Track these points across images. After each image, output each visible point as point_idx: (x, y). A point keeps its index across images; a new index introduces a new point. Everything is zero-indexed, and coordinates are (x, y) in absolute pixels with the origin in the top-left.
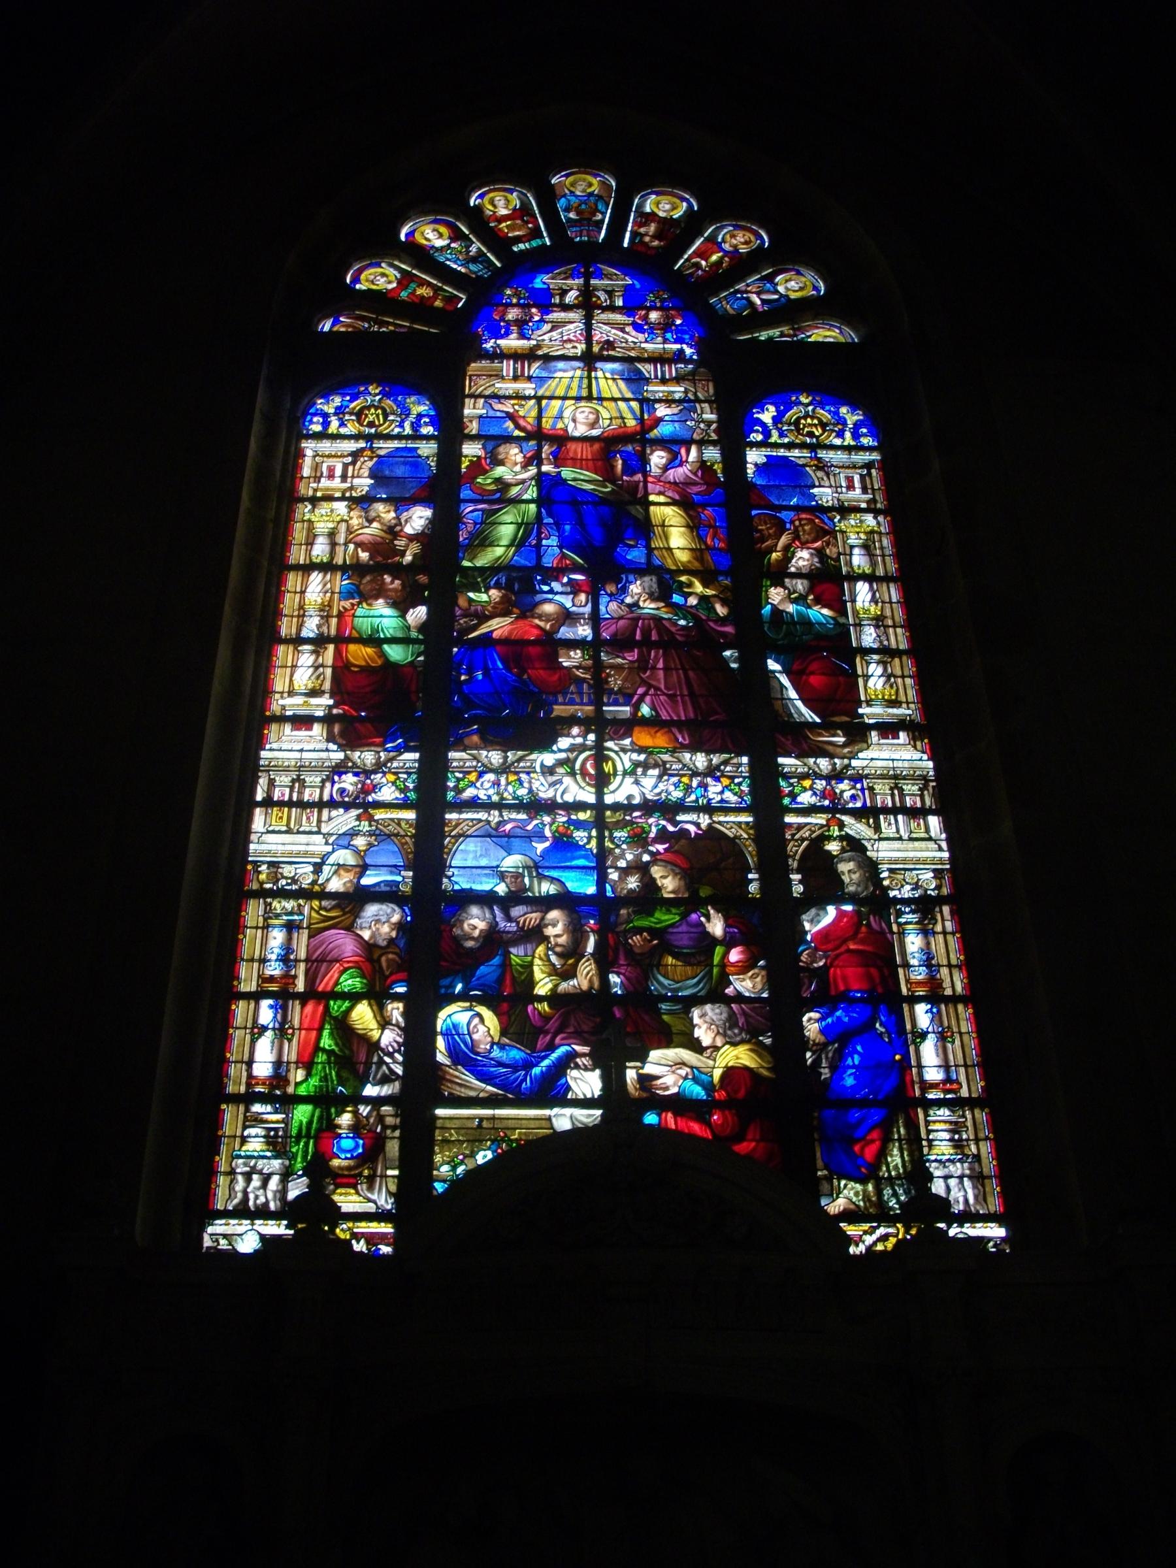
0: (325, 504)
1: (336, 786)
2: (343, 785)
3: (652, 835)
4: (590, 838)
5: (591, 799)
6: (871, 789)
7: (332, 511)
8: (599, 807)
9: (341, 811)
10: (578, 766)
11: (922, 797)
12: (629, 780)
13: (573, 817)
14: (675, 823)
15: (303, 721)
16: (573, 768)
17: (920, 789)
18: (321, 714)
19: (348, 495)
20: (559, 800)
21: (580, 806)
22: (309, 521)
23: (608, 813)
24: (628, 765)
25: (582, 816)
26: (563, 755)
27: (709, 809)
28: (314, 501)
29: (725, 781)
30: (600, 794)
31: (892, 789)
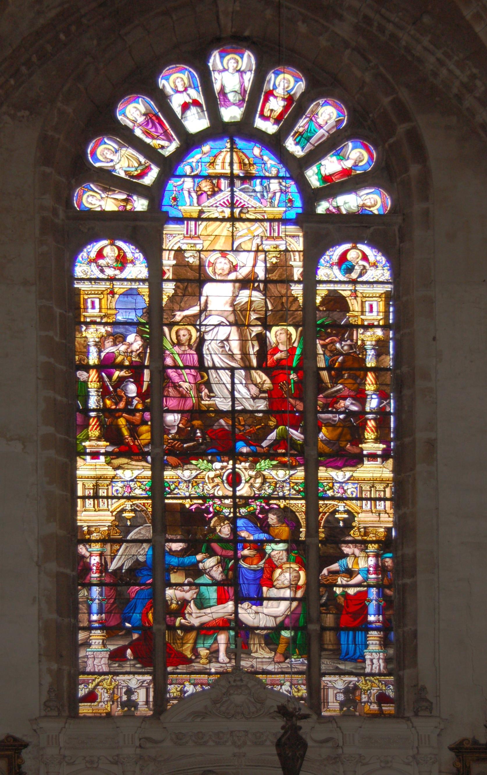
0: (92, 326)
1: (114, 489)
2: (117, 488)
3: (258, 511)
4: (230, 513)
5: (230, 494)
7: (97, 330)
8: (234, 497)
9: (116, 500)
10: (224, 478)
12: (247, 485)
14: (268, 504)
15: (95, 455)
16: (222, 479)
18: (103, 451)
19: (104, 320)
20: (216, 495)
21: (227, 497)
22: (86, 337)
23: (237, 500)
24: (247, 477)
25: (228, 501)
27: (284, 498)
28: (87, 324)
29: (292, 485)
30: (234, 491)
31: (371, 487)
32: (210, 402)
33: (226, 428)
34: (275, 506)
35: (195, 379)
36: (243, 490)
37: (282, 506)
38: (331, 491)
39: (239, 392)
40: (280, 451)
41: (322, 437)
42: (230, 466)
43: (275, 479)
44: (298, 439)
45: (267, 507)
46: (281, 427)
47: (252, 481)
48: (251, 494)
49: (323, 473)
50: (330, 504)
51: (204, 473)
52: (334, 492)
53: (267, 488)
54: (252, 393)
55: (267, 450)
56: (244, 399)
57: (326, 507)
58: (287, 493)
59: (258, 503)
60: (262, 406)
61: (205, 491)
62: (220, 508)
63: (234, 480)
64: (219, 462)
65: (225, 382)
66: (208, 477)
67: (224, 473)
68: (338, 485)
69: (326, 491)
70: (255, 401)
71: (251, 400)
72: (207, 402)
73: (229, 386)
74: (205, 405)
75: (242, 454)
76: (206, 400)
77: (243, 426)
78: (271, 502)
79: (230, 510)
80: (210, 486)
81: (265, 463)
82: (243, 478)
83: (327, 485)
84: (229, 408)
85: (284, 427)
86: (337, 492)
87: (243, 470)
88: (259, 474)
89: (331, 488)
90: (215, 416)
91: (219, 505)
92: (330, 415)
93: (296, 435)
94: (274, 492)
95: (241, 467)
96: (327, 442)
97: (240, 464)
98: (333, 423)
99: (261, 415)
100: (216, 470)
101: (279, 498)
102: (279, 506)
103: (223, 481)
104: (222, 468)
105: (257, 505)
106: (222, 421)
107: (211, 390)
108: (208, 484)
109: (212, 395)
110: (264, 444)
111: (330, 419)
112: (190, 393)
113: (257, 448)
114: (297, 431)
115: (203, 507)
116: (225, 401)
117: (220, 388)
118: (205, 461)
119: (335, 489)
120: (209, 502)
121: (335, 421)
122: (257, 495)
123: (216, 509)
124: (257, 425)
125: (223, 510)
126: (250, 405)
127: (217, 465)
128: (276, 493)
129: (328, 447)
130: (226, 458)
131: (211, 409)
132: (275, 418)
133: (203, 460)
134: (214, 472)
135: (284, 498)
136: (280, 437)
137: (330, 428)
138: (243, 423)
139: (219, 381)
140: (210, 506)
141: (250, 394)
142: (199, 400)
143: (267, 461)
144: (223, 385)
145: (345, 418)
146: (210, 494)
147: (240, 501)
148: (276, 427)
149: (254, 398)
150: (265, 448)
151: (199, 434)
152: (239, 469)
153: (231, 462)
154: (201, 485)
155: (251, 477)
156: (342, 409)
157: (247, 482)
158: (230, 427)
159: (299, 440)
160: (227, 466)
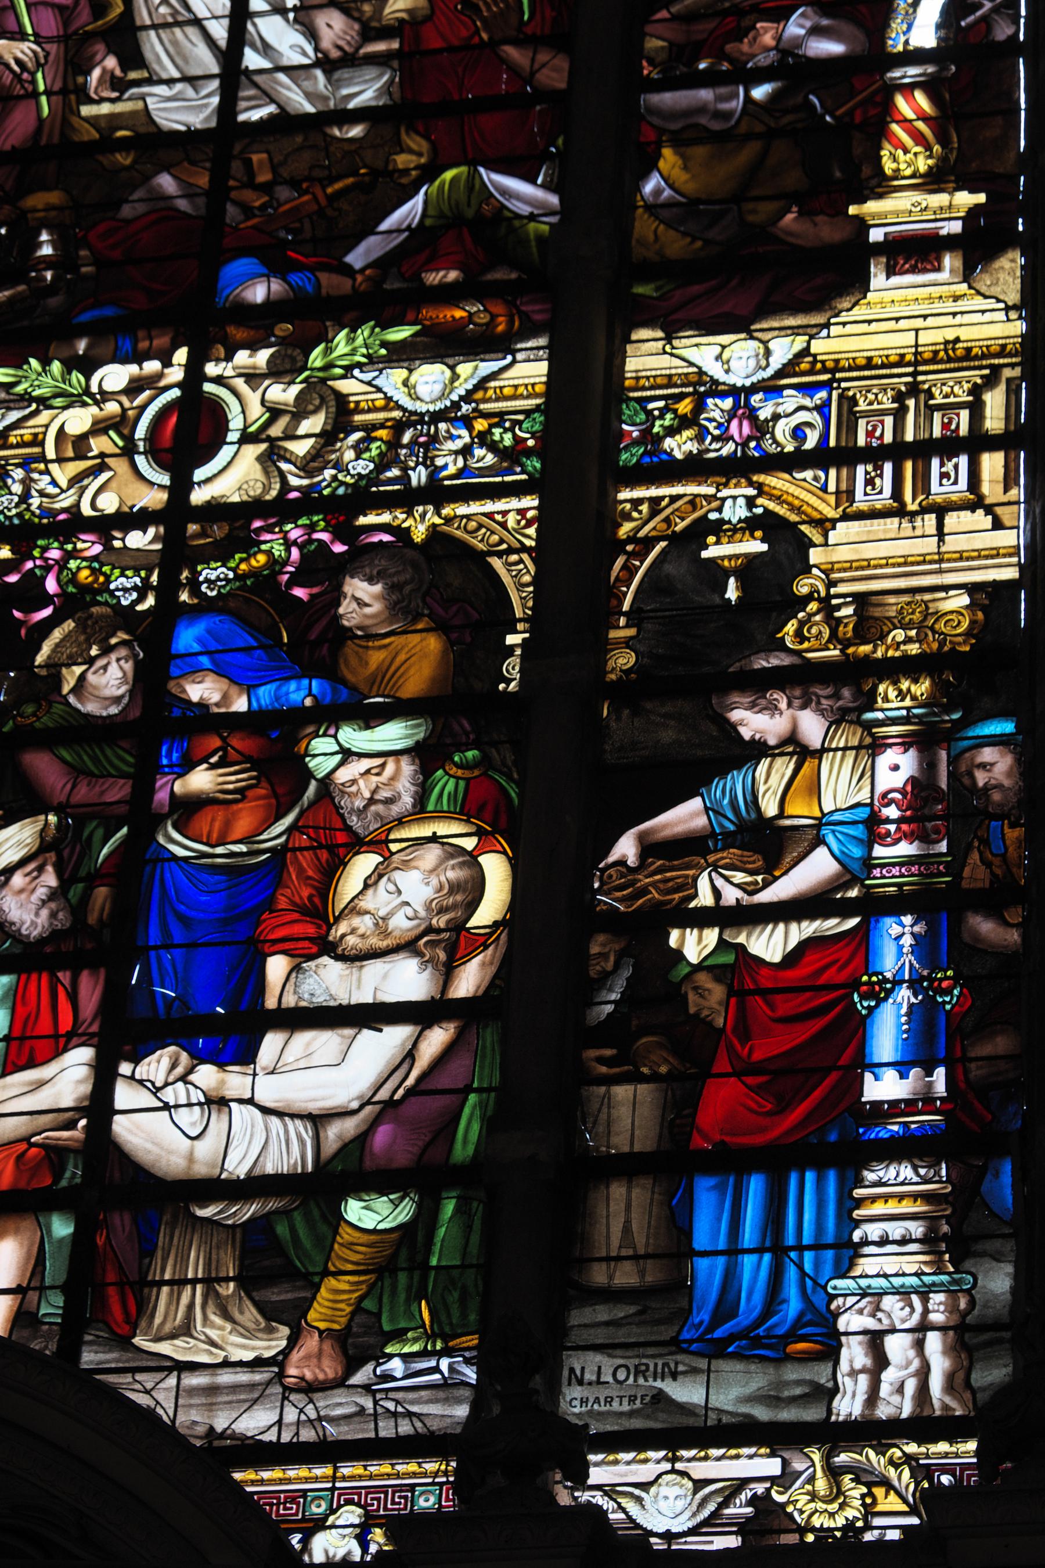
6: (848, 402)
11: (976, 408)
13: (117, 544)
17: (976, 391)
20: (86, 511)
24: (256, 411)
25: (136, 540)
26: (112, 407)
27: (437, 493)
30: (181, 486)
31: (899, 398)
32: (120, 107)
33: (182, 204)
34: (386, 538)
35: (66, 24)
36: (231, 476)
37: (419, 533)
38: (687, 433)
39: (266, 49)
40: (433, 278)
41: (657, 192)
42: (175, 374)
43: (399, 407)
44: (525, 210)
45: (339, 548)
46: (449, 175)
47: (276, 430)
48: (267, 488)
49: (647, 357)
50: (674, 499)
51: (45, 416)
52: (700, 438)
53: (349, 455)
54: (326, 44)
55: (368, 279)
56: (281, 77)
57: (654, 513)
58: (452, 470)
59: (295, 534)
60: (369, 94)
61: (35, 502)
62: (93, 571)
63: (191, 433)
64: (124, 361)
65: (201, 12)
66: (62, 428)
67: (143, 408)
68: (728, 403)
69: (659, 439)
70: (337, 75)
71: (319, 73)
72: (105, 108)
73: (219, 31)
74: (93, 121)
75: (246, 313)
76: (102, 100)
77: (266, 188)
78: (370, 519)
79: (146, 581)
80: (62, 474)
81: (350, 340)
82: (236, 423)
83: (663, 411)
84: (207, 119)
85: (463, 169)
86: (715, 439)
87: (240, 383)
88: (317, 392)
89: (685, 422)
90: (135, 162)
91: (95, 558)
92: (705, 95)
93: (523, 192)
94: (382, 464)
95: (229, 373)
96: (681, 212)
97: (229, 358)
98: (716, 126)
99: (356, 131)
100: (105, 396)
101: (408, 498)
102: (402, 534)
103: (129, 451)
104: (134, 388)
105: (288, 544)
106: (166, 182)
107: (133, 57)
108: (54, 468)
109: (133, 75)
110: (356, 258)
111: (702, 109)
112: (34, 82)
113: (324, 277)
114: (533, 181)
115: (13, 579)
116: (190, 92)
117: (175, 43)
118: (56, 366)
119: (711, 426)
120: (45, 549)
121: (727, 115)
122: (294, 495)
123: (73, 580)
124: (333, 180)
125: (108, 581)
126: (308, 96)
127: (114, 376)
128: (395, 472)
129: (685, 234)
130: (161, 341)
131: (121, 133)
132: (426, 137)
133: (46, 363)
134: (94, 410)
135: (437, 493)
136: (441, 215)
137: (700, 152)
138: (264, 177)
139: (175, 13)
140: (47, 569)
141: (317, 49)
142: (66, 104)
143: (363, 333)
144: (192, 32)
145: (774, 98)
146: (53, 513)
147: (203, 534)
148: (429, 173)
149: (327, 64)
150: (362, 270)
151: (47, 250)
152: (219, 380)
153: (181, 355)
154: (18, 474)
155: (275, 412)
156: (764, 60)
157: (247, 438)
158: (201, 201)
159: (532, 217)
160: (160, 376)
